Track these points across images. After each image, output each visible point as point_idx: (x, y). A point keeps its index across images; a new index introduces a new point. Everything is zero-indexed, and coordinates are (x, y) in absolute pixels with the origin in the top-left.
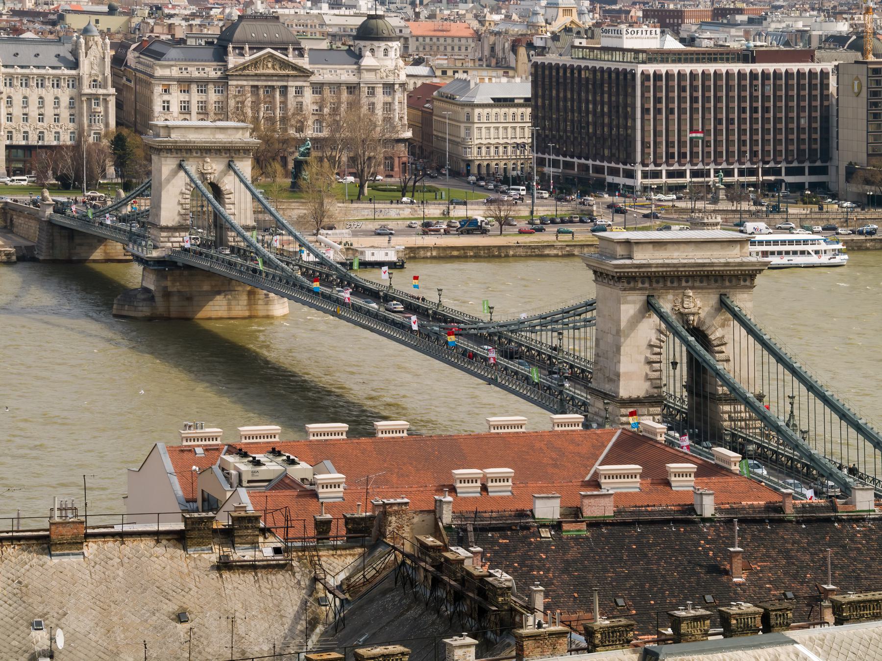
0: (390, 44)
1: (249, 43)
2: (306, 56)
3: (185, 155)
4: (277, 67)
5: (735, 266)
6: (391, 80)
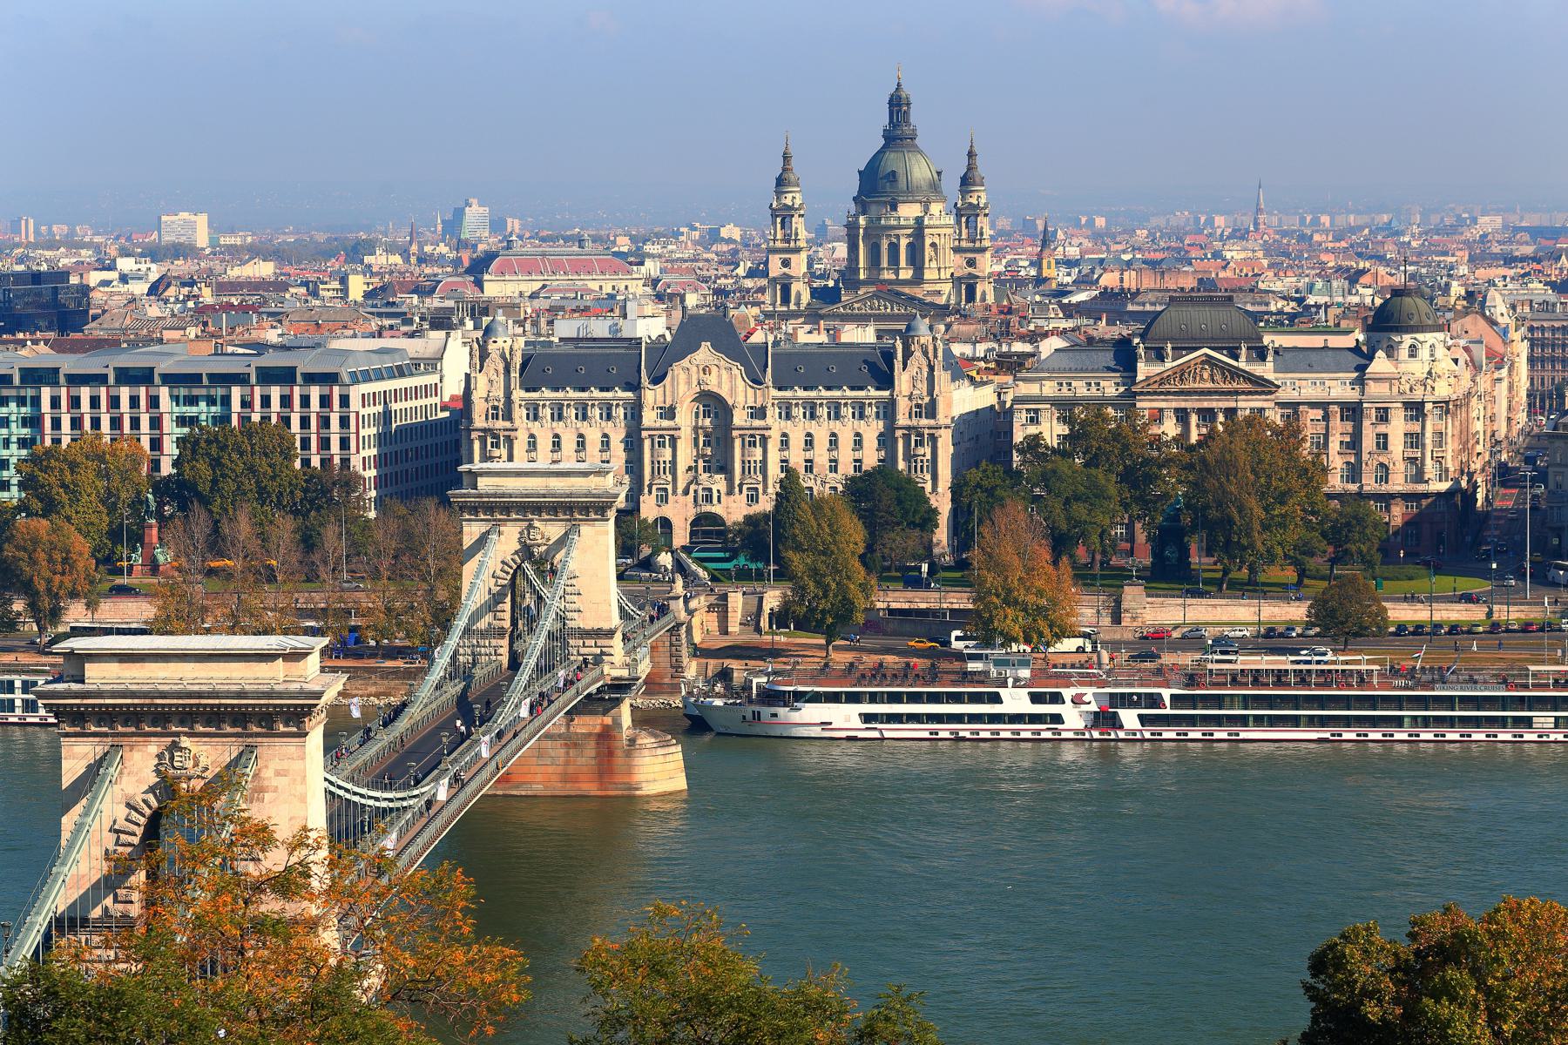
0: (1420, 336)
1: (1172, 340)
2: (1270, 358)
4: (1218, 377)
6: (1418, 395)
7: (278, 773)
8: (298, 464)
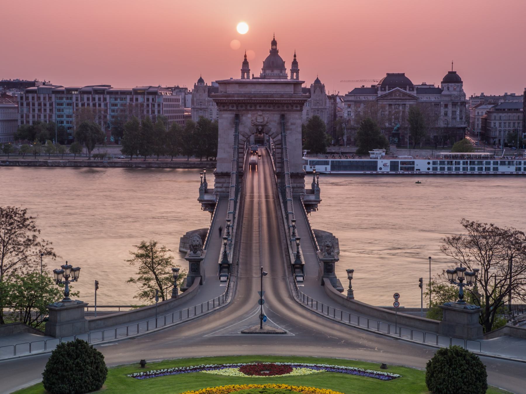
5: (287, 97)
7: (292, 124)
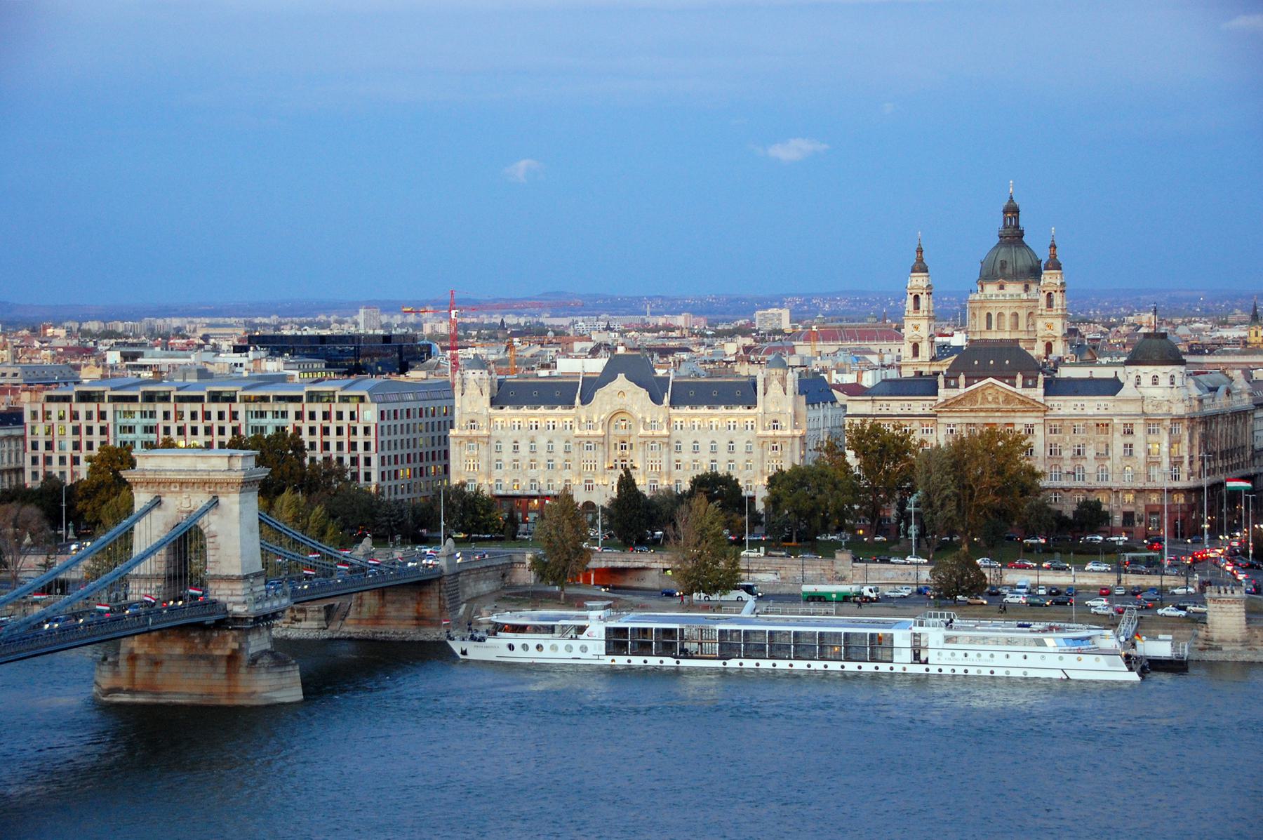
3: (162, 489)
8: (307, 461)
